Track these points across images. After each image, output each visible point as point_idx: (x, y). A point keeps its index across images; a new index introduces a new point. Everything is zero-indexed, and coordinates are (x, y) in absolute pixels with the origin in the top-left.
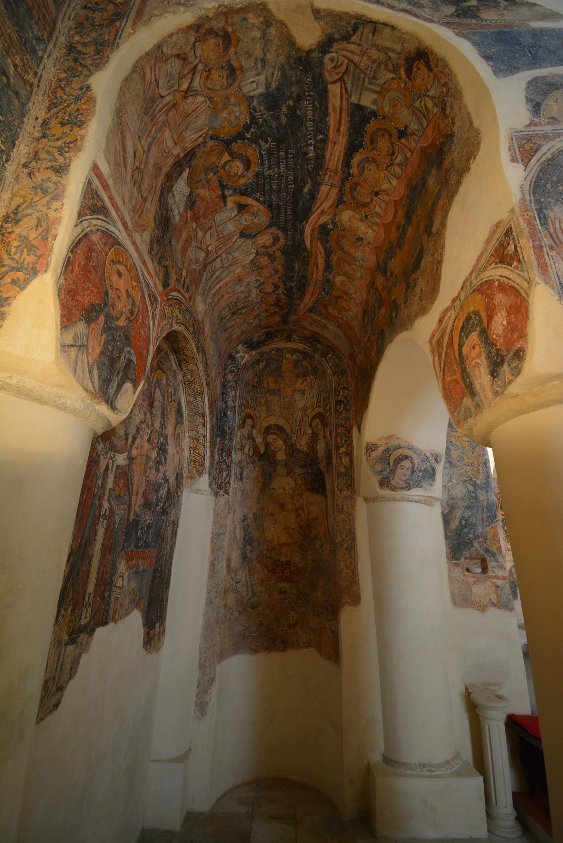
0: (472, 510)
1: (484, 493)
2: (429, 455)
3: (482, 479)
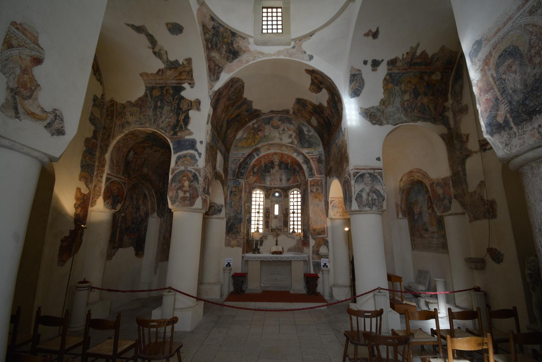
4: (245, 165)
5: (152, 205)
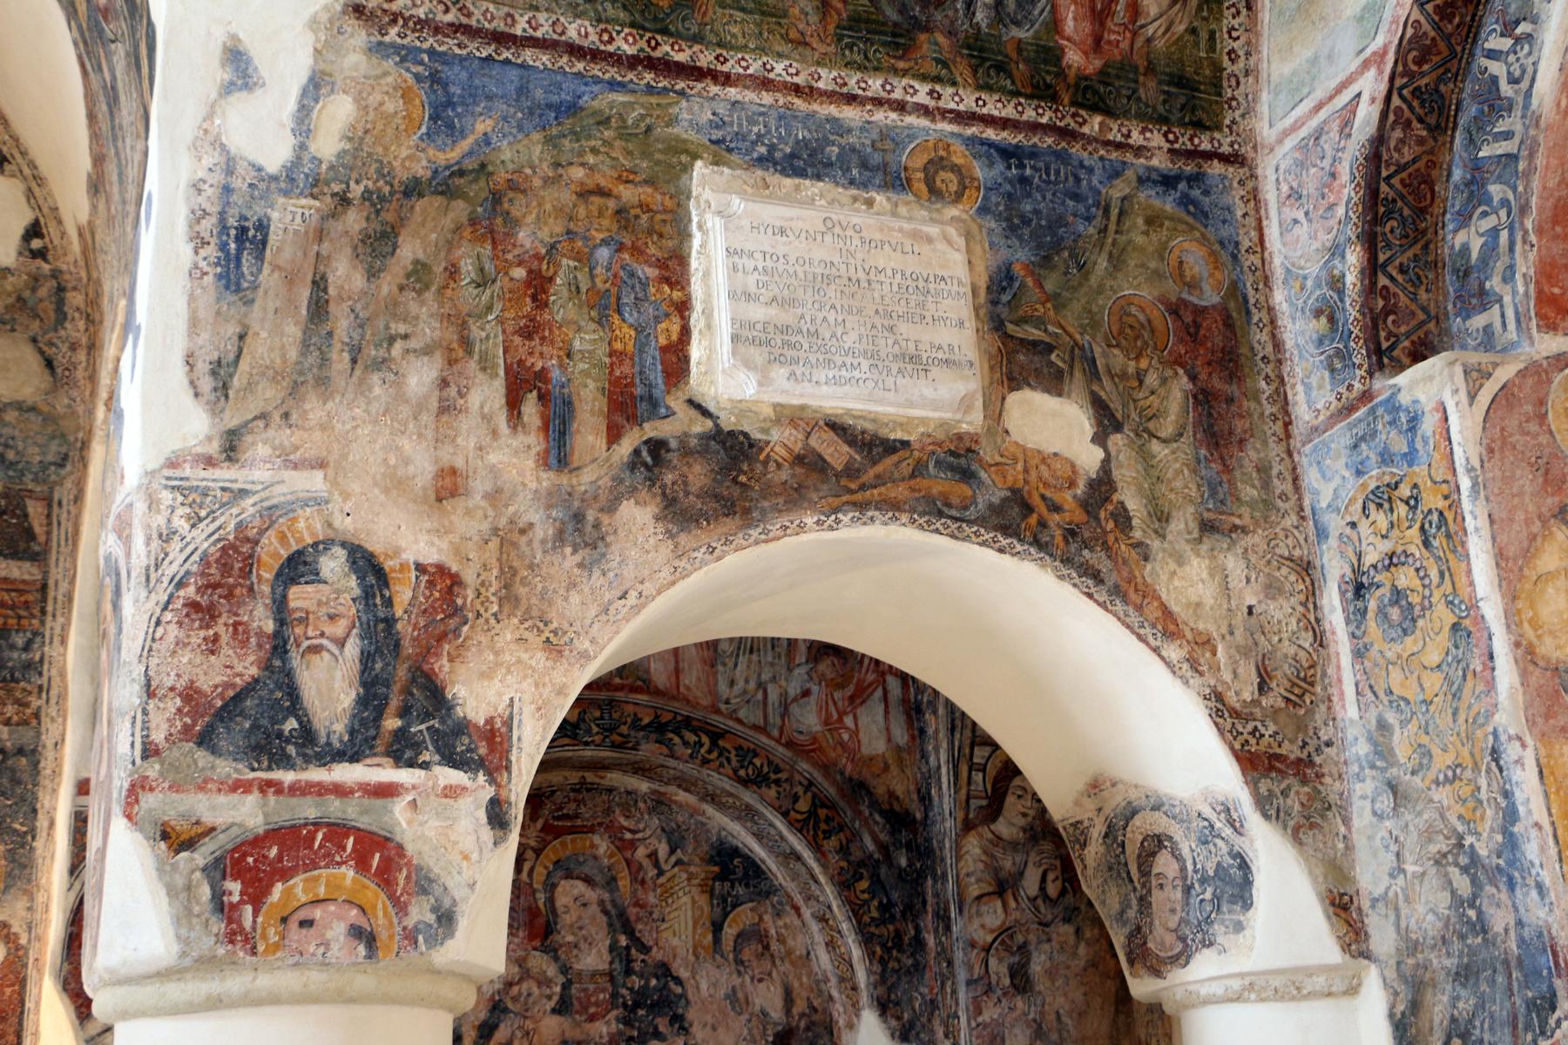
0: (1476, 984)
1: (1504, 896)
2: (1207, 812)
3: (1492, 830)
4: (1471, 142)
5: (831, 945)
